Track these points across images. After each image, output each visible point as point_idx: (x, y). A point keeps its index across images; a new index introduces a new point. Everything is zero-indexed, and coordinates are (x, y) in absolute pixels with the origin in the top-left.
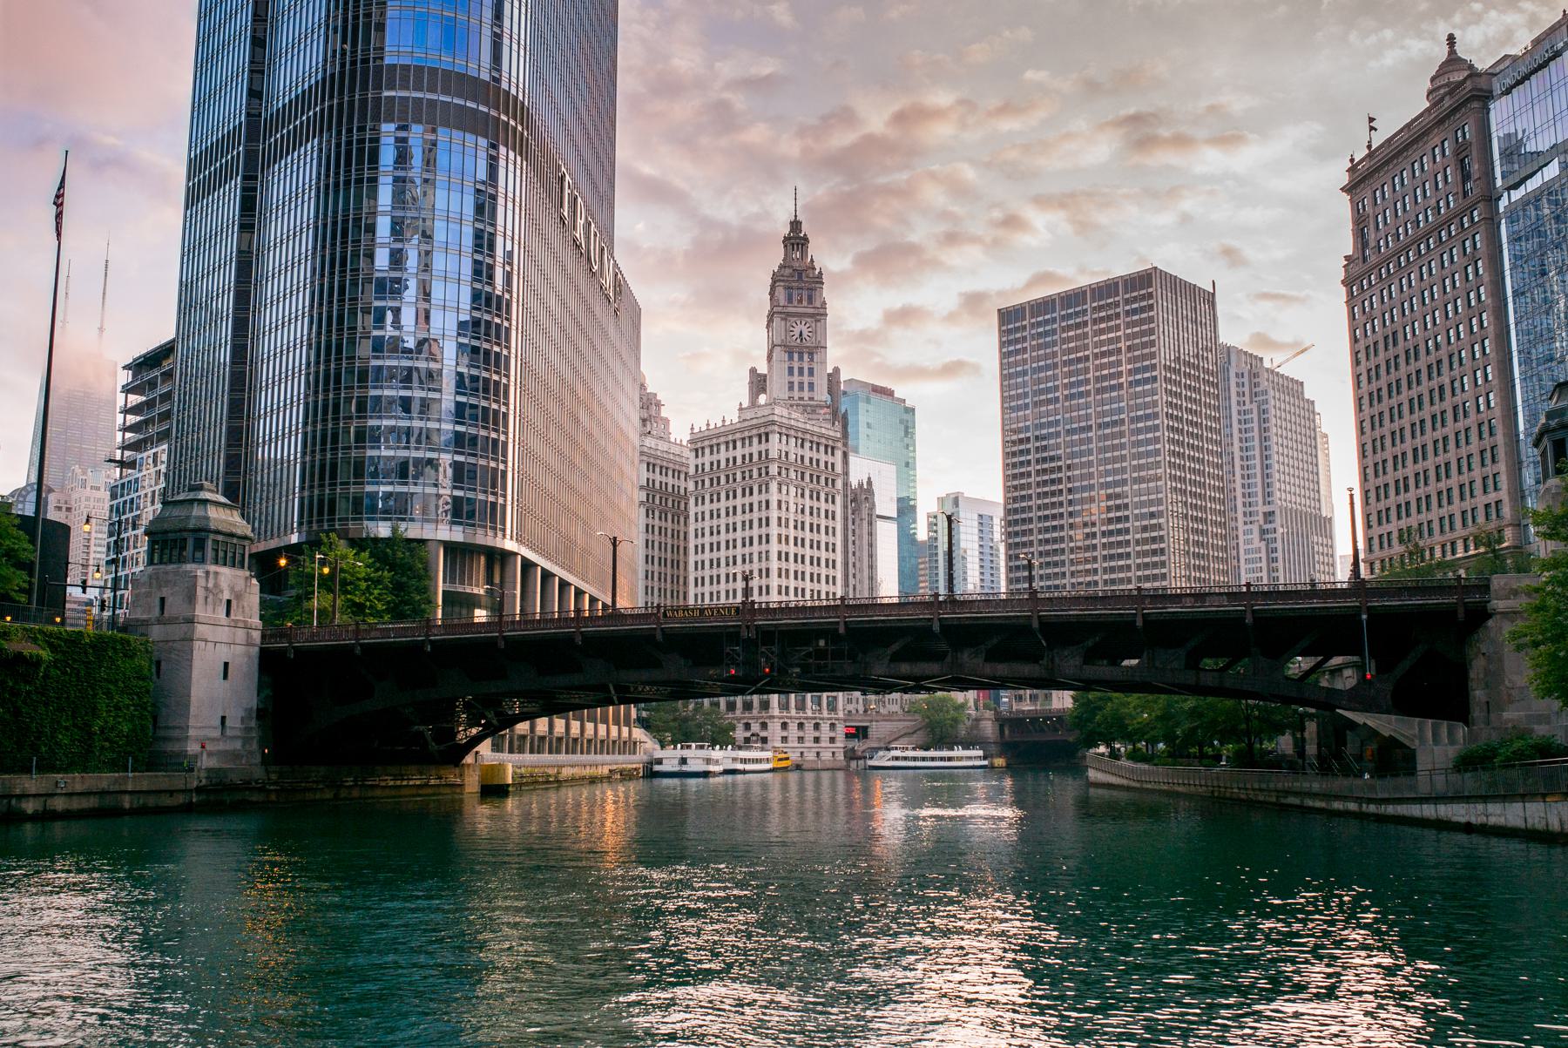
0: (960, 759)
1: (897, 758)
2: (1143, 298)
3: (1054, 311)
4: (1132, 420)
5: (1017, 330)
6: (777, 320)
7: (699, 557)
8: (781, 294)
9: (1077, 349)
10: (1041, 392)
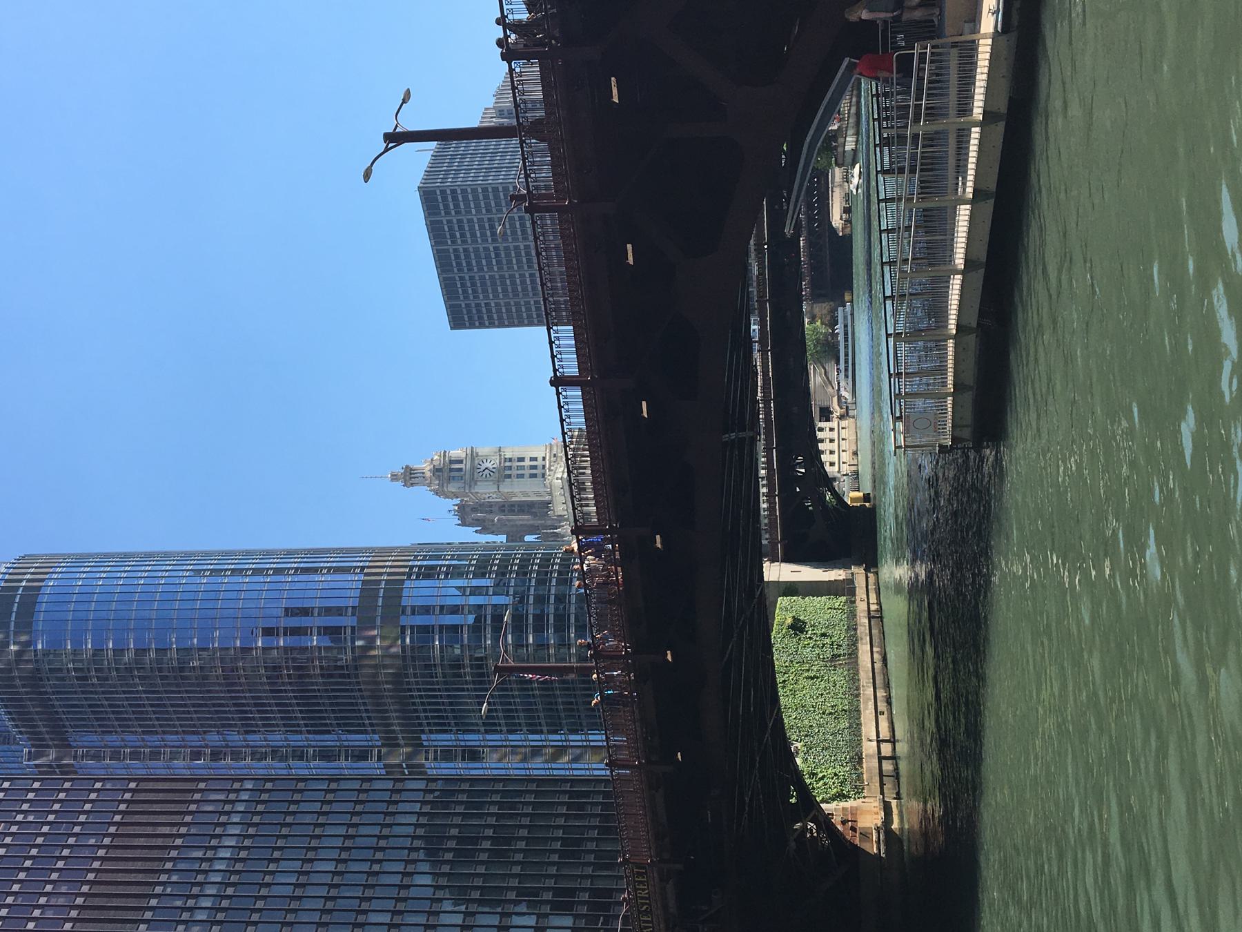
2: (444, 199)
9: (488, 257)
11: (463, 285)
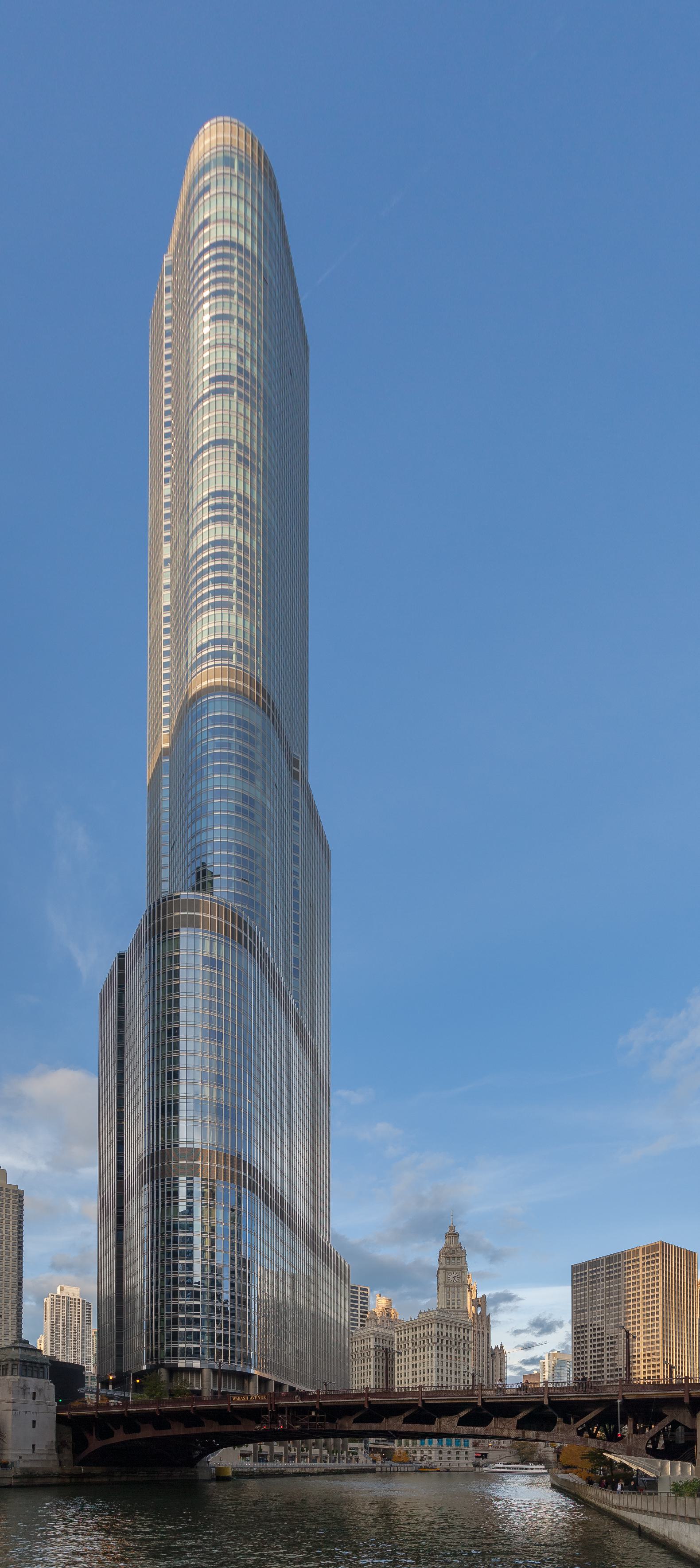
0: (532, 1469)
1: (498, 1468)
6: (441, 1272)
7: (399, 1379)
8: (443, 1259)
10: (594, 1304)
11: (598, 1270)
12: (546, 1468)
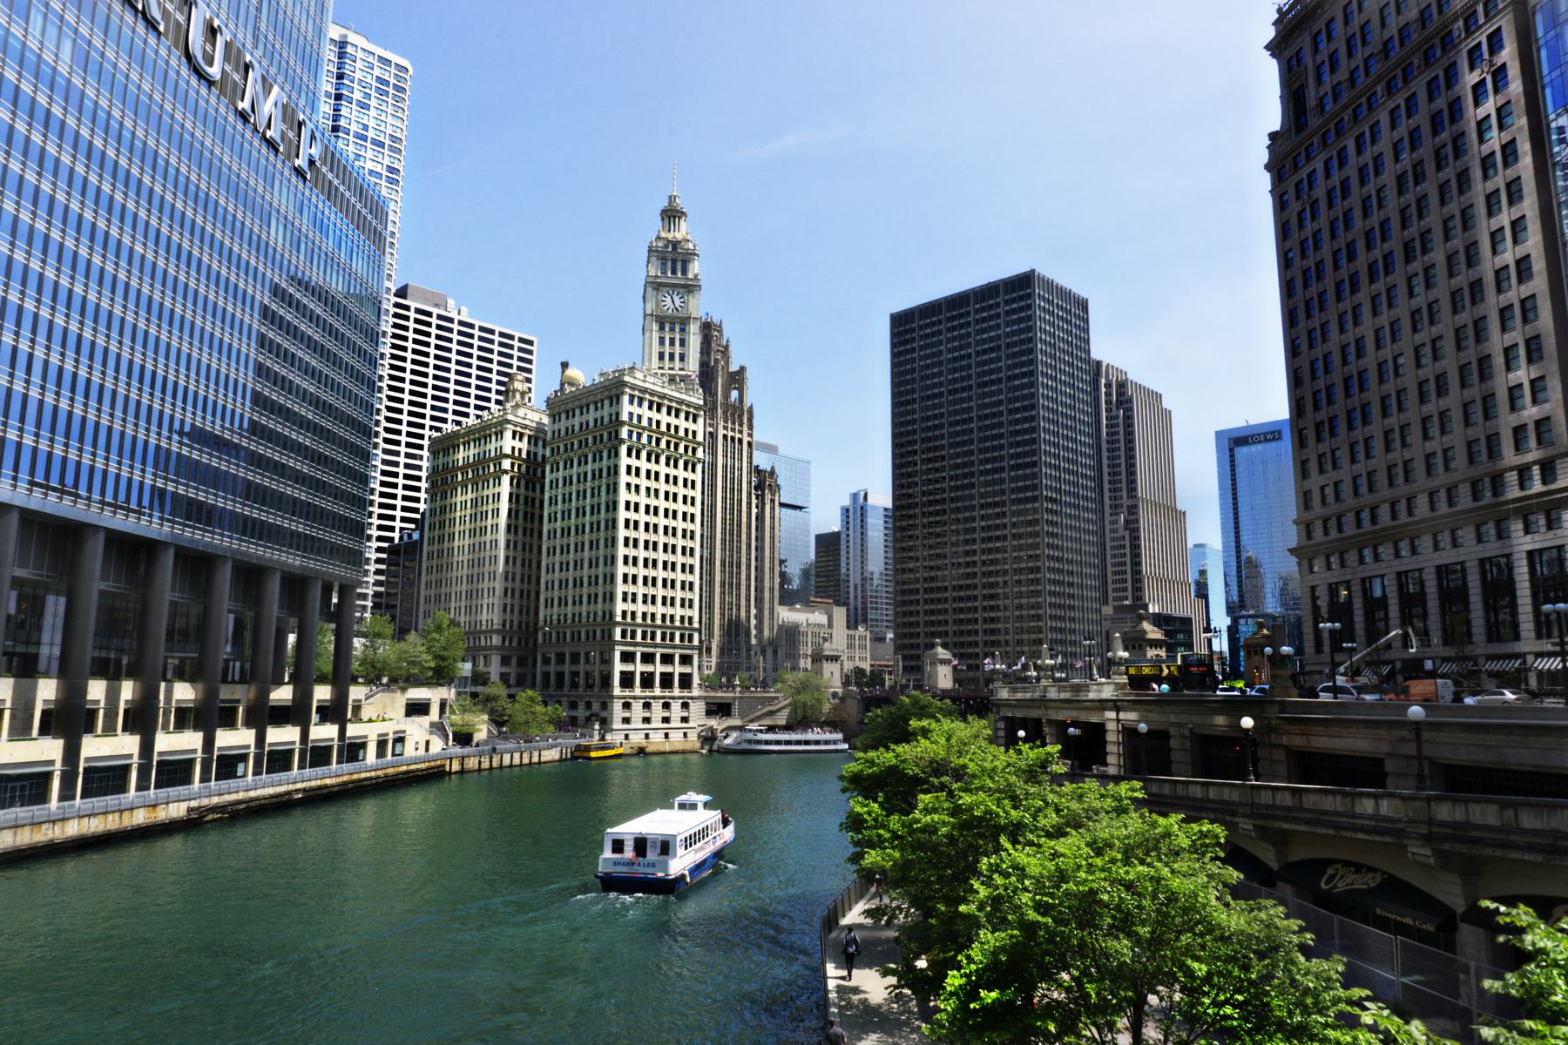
0: (817, 742)
2: (1021, 298)
3: (940, 313)
4: (1010, 412)
5: (907, 332)
9: (961, 348)
11: (933, 324)
12: (845, 740)
